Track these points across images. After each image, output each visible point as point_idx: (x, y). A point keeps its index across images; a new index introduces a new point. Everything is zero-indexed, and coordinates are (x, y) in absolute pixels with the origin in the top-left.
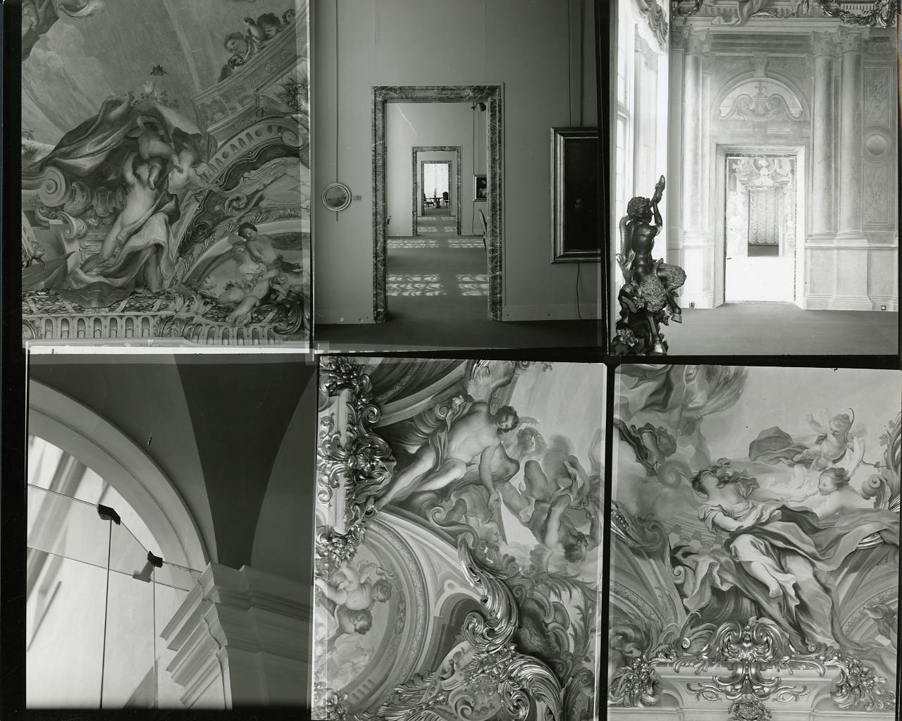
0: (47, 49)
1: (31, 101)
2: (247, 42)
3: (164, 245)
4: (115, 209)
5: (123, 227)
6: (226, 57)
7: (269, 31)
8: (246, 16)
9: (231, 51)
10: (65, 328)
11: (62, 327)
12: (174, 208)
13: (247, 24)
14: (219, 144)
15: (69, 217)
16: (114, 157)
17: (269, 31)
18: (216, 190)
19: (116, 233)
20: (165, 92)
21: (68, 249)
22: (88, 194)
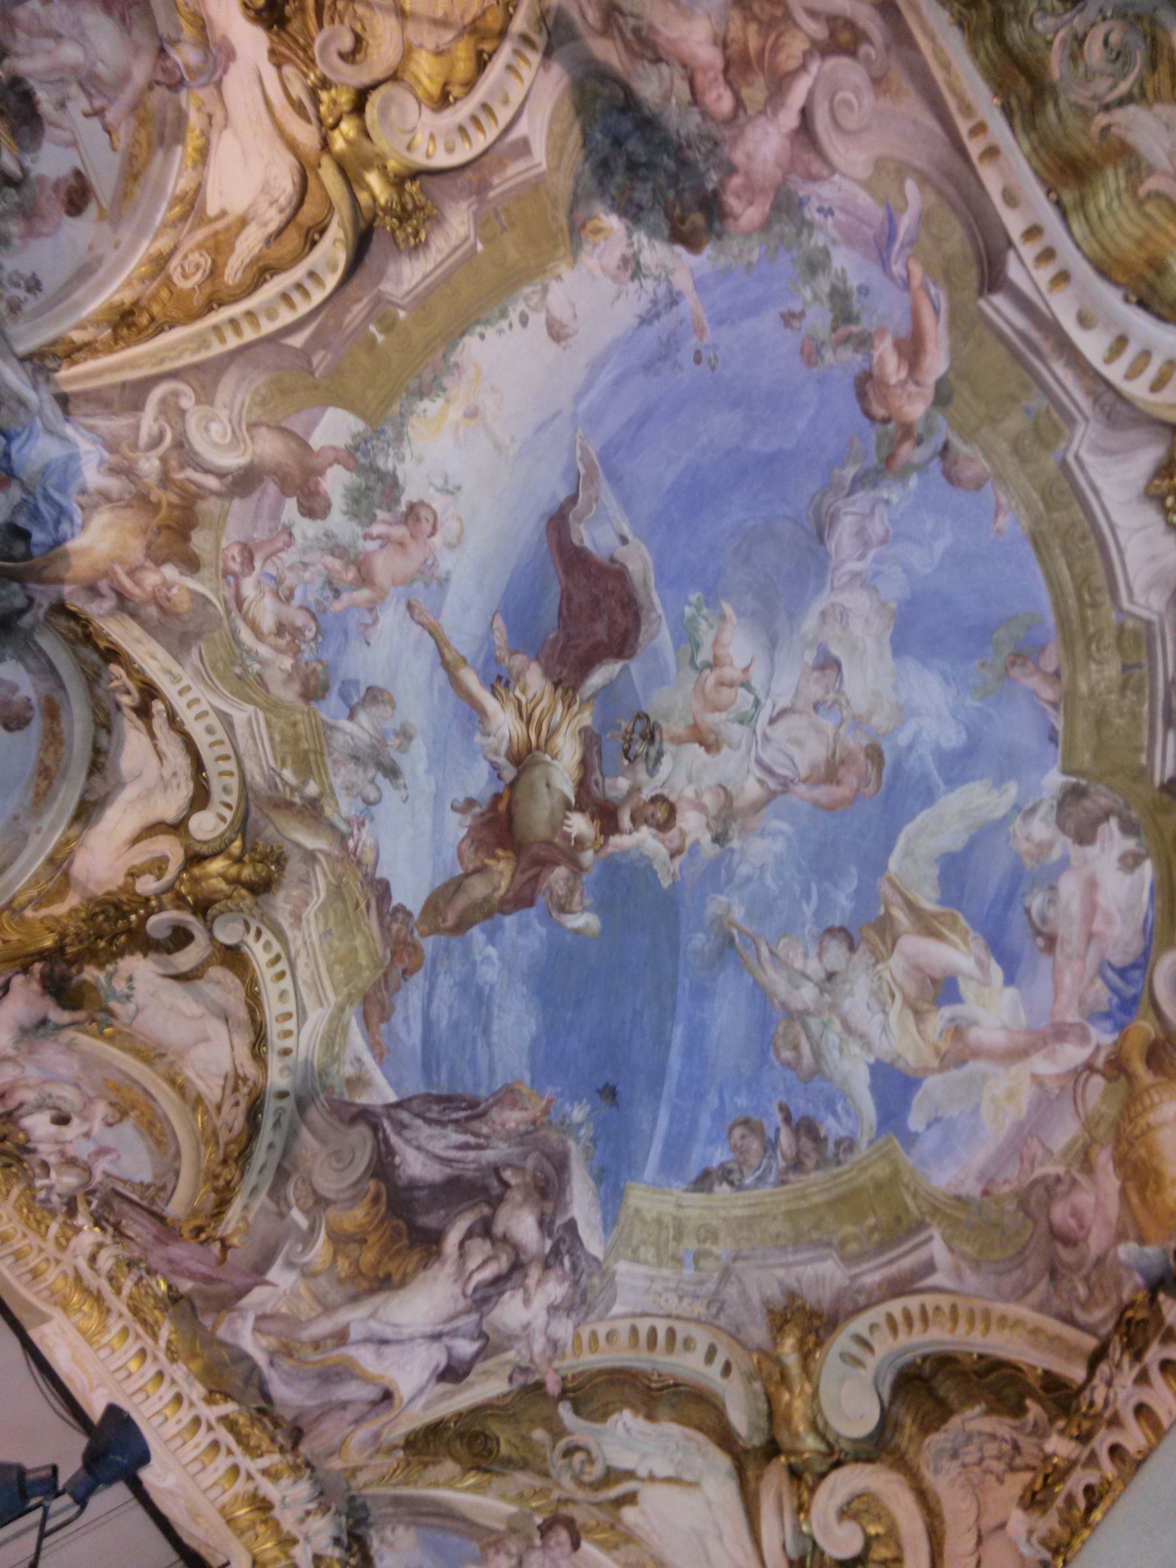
0: (491, 940)
2: (765, 1150)
3: (396, 1402)
4: (388, 1277)
5: (373, 1316)
6: (720, 1156)
8: (783, 1098)
9: (734, 1148)
10: (133, 1366)
11: (131, 1359)
13: (778, 1117)
14: (617, 1309)
16: (458, 1190)
18: (553, 1387)
19: (356, 1318)
21: (275, 1273)
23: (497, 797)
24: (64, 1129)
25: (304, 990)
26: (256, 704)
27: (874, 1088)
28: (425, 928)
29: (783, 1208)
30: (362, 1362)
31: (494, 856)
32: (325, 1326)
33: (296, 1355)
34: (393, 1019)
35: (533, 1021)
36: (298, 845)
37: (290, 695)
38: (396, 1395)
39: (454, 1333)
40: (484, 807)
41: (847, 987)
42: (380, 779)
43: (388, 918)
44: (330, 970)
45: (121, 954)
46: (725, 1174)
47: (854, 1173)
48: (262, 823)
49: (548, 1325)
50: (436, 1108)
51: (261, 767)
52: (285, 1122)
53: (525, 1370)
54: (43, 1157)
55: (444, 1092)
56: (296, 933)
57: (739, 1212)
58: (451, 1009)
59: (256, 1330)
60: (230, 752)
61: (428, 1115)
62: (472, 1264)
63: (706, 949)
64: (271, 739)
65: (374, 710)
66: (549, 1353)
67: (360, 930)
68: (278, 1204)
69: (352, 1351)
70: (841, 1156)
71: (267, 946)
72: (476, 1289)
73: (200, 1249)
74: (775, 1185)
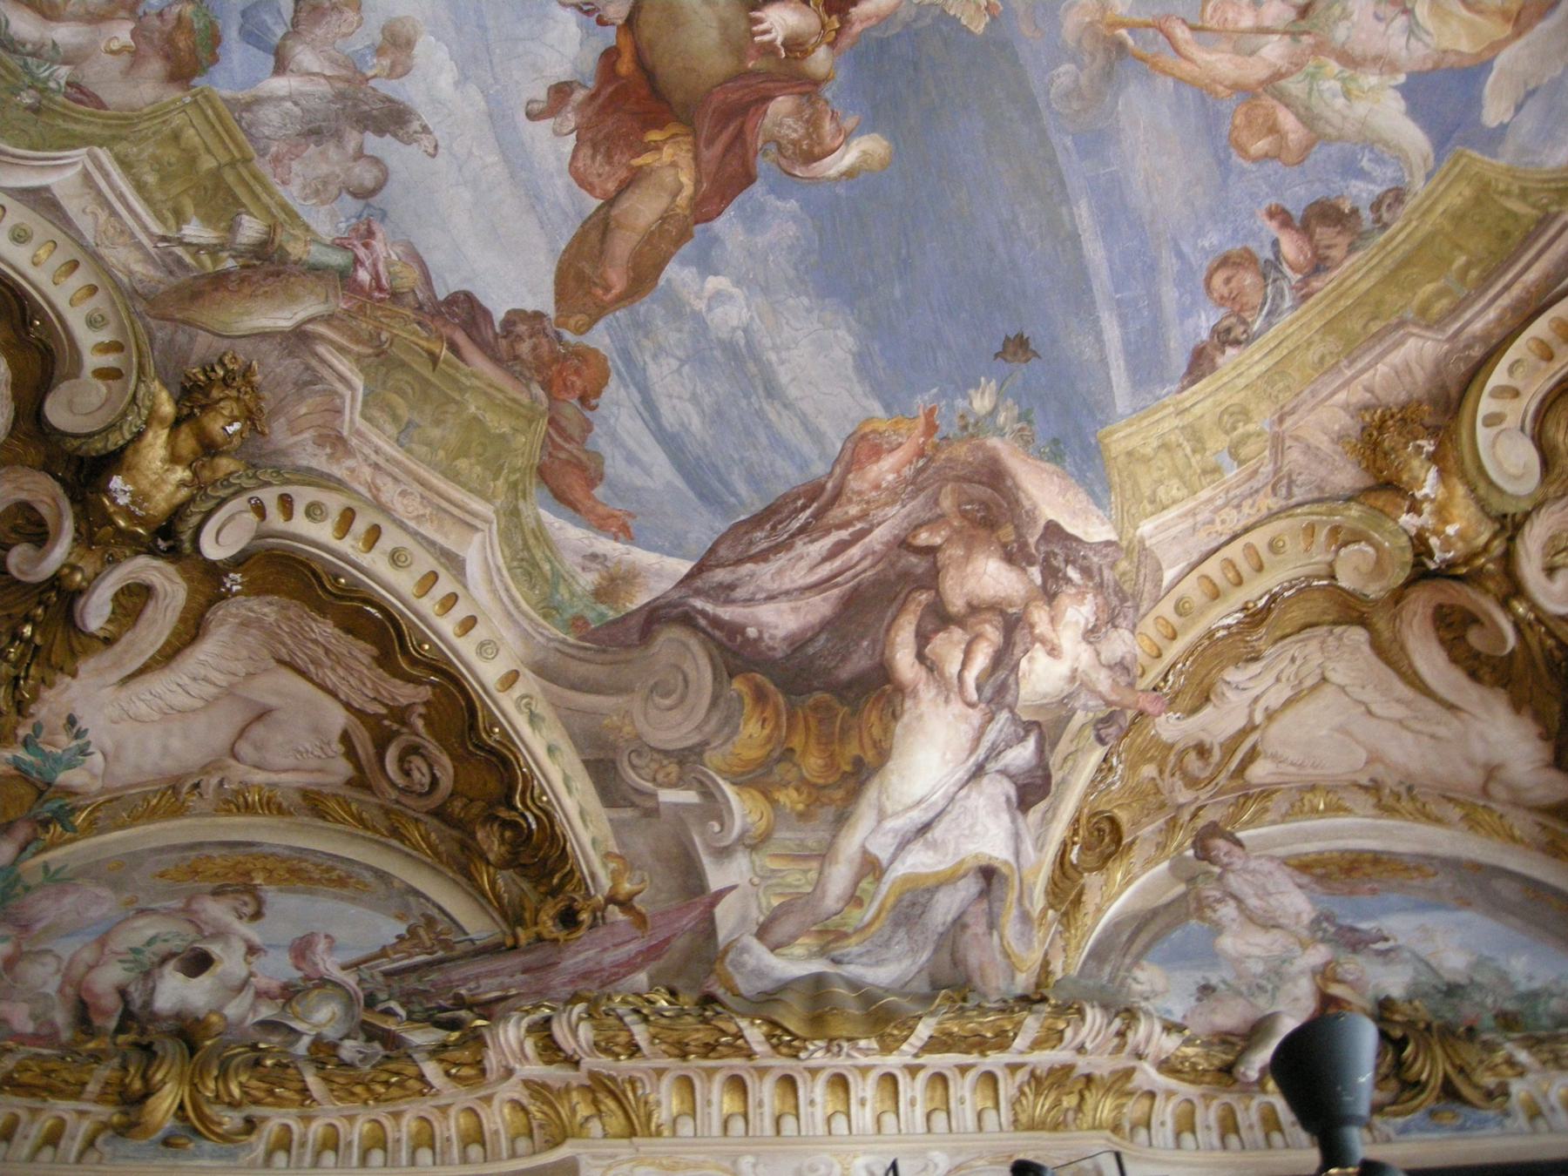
0: (707, 267)
1: (640, 422)
2: (1265, 277)
3: (1004, 870)
4: (858, 762)
6: (1205, 322)
7: (1329, 247)
8: (1273, 201)
12: (1034, 762)
13: (1272, 227)
14: (1169, 575)
15: (721, 782)
16: (864, 606)
17: (1329, 247)
19: (866, 833)
20: (1030, 411)
21: (716, 878)
22: (778, 715)
23: (609, 57)
24: (217, 969)
25: (428, 530)
26: (85, 140)
27: (1415, 110)
28: (581, 318)
29: (1317, 325)
30: (923, 870)
31: (647, 148)
32: (840, 877)
33: (850, 930)
34: (609, 470)
35: (842, 333)
36: (264, 335)
37: (147, 89)
38: (997, 864)
39: (995, 752)
40: (591, 84)
41: (1337, 10)
42: (374, 143)
43: (503, 343)
44: (453, 476)
45: (36, 697)
46: (1224, 337)
47: (1414, 224)
48: (181, 338)
49: (1098, 654)
50: (759, 534)
51: (140, 246)
52: (541, 708)
53: (1108, 720)
54: (251, 1019)
55: (759, 506)
56: (351, 463)
57: (1262, 368)
58: (695, 399)
59: (774, 948)
60: (76, 254)
61: (754, 550)
62: (953, 668)
63: (1084, 80)
64: (140, 187)
65: (319, 32)
66: (1123, 680)
67: (462, 389)
68: (633, 805)
69: (900, 869)
70: (1386, 216)
71: (314, 511)
72: (979, 688)
73: (601, 932)
74: (1294, 308)
